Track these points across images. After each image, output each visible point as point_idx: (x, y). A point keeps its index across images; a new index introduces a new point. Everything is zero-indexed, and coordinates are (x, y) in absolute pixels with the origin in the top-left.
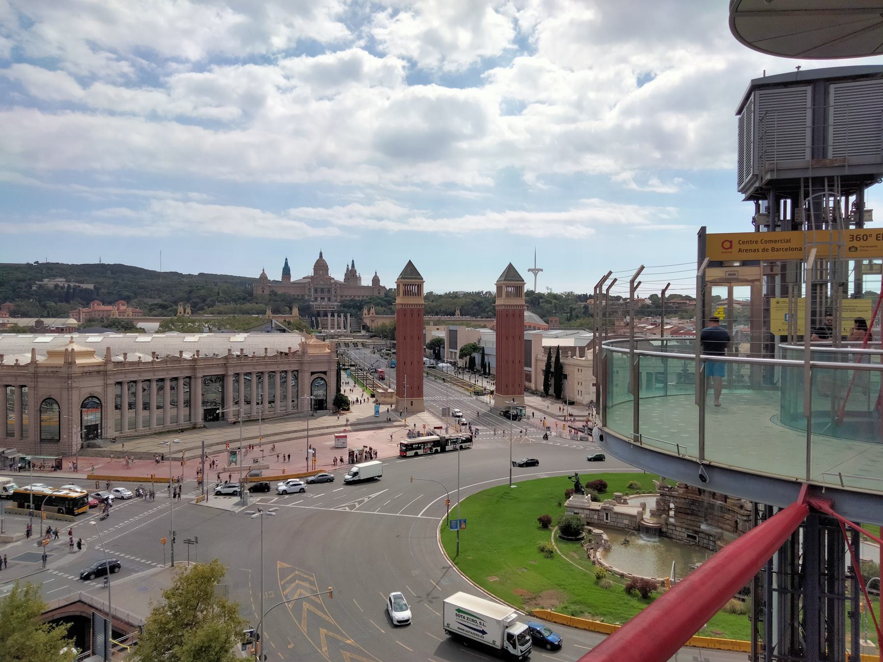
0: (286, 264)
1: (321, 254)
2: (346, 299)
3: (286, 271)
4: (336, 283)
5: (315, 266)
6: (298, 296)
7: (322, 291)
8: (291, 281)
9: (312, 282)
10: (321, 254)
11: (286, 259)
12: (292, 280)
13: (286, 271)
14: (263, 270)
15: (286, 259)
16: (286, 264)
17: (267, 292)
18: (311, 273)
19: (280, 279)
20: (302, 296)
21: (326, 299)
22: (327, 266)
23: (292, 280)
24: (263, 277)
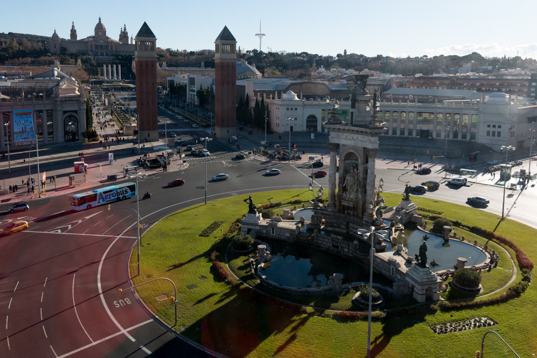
0: (73, 26)
1: (100, 19)
2: (120, 54)
3: (73, 33)
4: (113, 42)
5: (95, 28)
6: (83, 51)
7: (101, 46)
8: (78, 39)
9: (94, 40)
10: (100, 19)
11: (73, 23)
12: (79, 38)
13: (73, 33)
14: (55, 31)
15: (73, 23)
16: (73, 26)
17: (58, 48)
18: (92, 33)
19: (69, 38)
20: (86, 51)
21: (105, 54)
22: (105, 29)
23: (79, 38)
24: (55, 35)
